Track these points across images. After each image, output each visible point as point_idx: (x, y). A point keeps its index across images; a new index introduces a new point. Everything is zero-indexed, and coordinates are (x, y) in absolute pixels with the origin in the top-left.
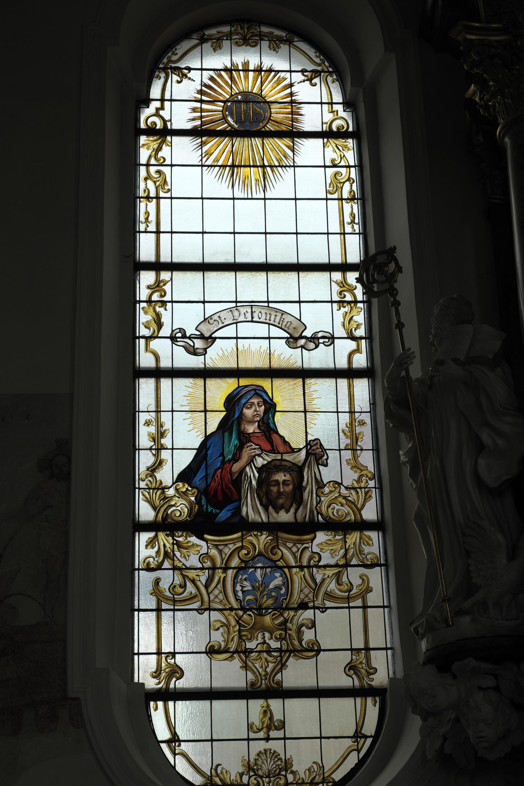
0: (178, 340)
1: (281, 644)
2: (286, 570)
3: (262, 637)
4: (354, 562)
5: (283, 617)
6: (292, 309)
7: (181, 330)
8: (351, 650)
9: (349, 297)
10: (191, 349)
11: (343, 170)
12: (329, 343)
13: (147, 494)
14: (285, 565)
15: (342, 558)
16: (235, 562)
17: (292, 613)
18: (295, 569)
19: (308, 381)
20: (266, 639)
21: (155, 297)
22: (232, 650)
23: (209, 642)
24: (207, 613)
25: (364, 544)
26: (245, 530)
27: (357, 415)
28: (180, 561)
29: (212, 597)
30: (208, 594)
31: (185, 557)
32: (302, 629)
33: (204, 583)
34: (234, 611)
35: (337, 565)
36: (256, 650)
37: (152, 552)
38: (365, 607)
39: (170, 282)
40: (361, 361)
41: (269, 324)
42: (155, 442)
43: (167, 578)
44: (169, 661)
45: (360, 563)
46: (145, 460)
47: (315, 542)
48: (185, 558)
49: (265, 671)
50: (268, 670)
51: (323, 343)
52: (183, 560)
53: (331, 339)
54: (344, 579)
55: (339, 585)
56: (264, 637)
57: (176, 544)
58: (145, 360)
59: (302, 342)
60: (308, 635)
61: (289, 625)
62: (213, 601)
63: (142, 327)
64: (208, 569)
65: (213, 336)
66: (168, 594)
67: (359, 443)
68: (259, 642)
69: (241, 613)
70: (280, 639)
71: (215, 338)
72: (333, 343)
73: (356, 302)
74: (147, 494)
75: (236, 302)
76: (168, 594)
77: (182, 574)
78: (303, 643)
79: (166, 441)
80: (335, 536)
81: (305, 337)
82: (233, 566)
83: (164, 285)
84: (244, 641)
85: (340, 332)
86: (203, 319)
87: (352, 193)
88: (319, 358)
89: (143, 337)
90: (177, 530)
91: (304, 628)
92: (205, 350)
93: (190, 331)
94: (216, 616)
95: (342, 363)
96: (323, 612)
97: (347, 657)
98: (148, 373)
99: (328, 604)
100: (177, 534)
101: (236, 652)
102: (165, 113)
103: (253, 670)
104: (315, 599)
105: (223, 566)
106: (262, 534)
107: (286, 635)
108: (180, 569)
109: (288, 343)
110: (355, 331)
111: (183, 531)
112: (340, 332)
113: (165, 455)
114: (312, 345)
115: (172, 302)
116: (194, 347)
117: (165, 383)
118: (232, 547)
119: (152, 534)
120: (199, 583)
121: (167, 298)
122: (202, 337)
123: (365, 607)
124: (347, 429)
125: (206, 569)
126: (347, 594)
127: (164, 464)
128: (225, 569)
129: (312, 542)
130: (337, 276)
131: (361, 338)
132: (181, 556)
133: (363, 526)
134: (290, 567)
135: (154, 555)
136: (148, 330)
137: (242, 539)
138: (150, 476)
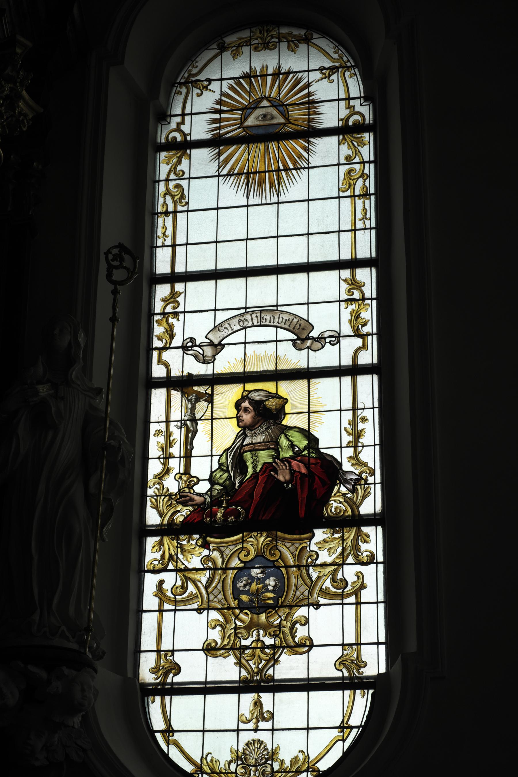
1: (275, 641)
2: (283, 570)
6: (301, 311)
7: (192, 340)
8: (343, 645)
9: (357, 295)
11: (357, 167)
13: (153, 500)
14: (283, 565)
16: (235, 563)
19: (313, 381)
20: (261, 636)
21: (169, 309)
23: (206, 640)
24: (206, 612)
27: (359, 412)
28: (183, 564)
29: (211, 597)
30: (208, 594)
31: (187, 559)
33: (204, 583)
38: (358, 603)
40: (367, 358)
42: (163, 451)
43: (170, 579)
46: (154, 467)
47: (314, 541)
49: (258, 667)
50: (260, 666)
51: (330, 342)
52: (186, 563)
54: (340, 576)
56: (258, 635)
57: (180, 547)
58: (158, 371)
60: (301, 632)
62: (212, 601)
63: (155, 339)
64: (209, 569)
65: (222, 343)
66: (169, 594)
67: (360, 440)
68: (254, 639)
69: (237, 611)
71: (224, 345)
72: (339, 341)
73: (364, 299)
76: (169, 594)
78: (296, 640)
80: (333, 535)
84: (239, 638)
86: (213, 327)
87: (365, 189)
88: (326, 357)
89: (156, 349)
90: (181, 535)
91: (298, 626)
92: (214, 357)
94: (214, 615)
95: (347, 361)
100: (181, 538)
102: (185, 128)
103: (246, 668)
104: (310, 597)
105: (224, 567)
107: (280, 632)
109: (294, 345)
110: (362, 327)
112: (347, 330)
114: (318, 345)
115: (185, 312)
116: (203, 355)
118: (233, 548)
119: (158, 539)
120: (199, 584)
121: (181, 309)
122: (211, 344)
123: (358, 603)
124: (349, 426)
126: (341, 591)
127: (171, 471)
128: (225, 570)
129: (310, 542)
130: (346, 274)
132: (183, 558)
134: (287, 567)
135: (159, 558)
138: (158, 483)
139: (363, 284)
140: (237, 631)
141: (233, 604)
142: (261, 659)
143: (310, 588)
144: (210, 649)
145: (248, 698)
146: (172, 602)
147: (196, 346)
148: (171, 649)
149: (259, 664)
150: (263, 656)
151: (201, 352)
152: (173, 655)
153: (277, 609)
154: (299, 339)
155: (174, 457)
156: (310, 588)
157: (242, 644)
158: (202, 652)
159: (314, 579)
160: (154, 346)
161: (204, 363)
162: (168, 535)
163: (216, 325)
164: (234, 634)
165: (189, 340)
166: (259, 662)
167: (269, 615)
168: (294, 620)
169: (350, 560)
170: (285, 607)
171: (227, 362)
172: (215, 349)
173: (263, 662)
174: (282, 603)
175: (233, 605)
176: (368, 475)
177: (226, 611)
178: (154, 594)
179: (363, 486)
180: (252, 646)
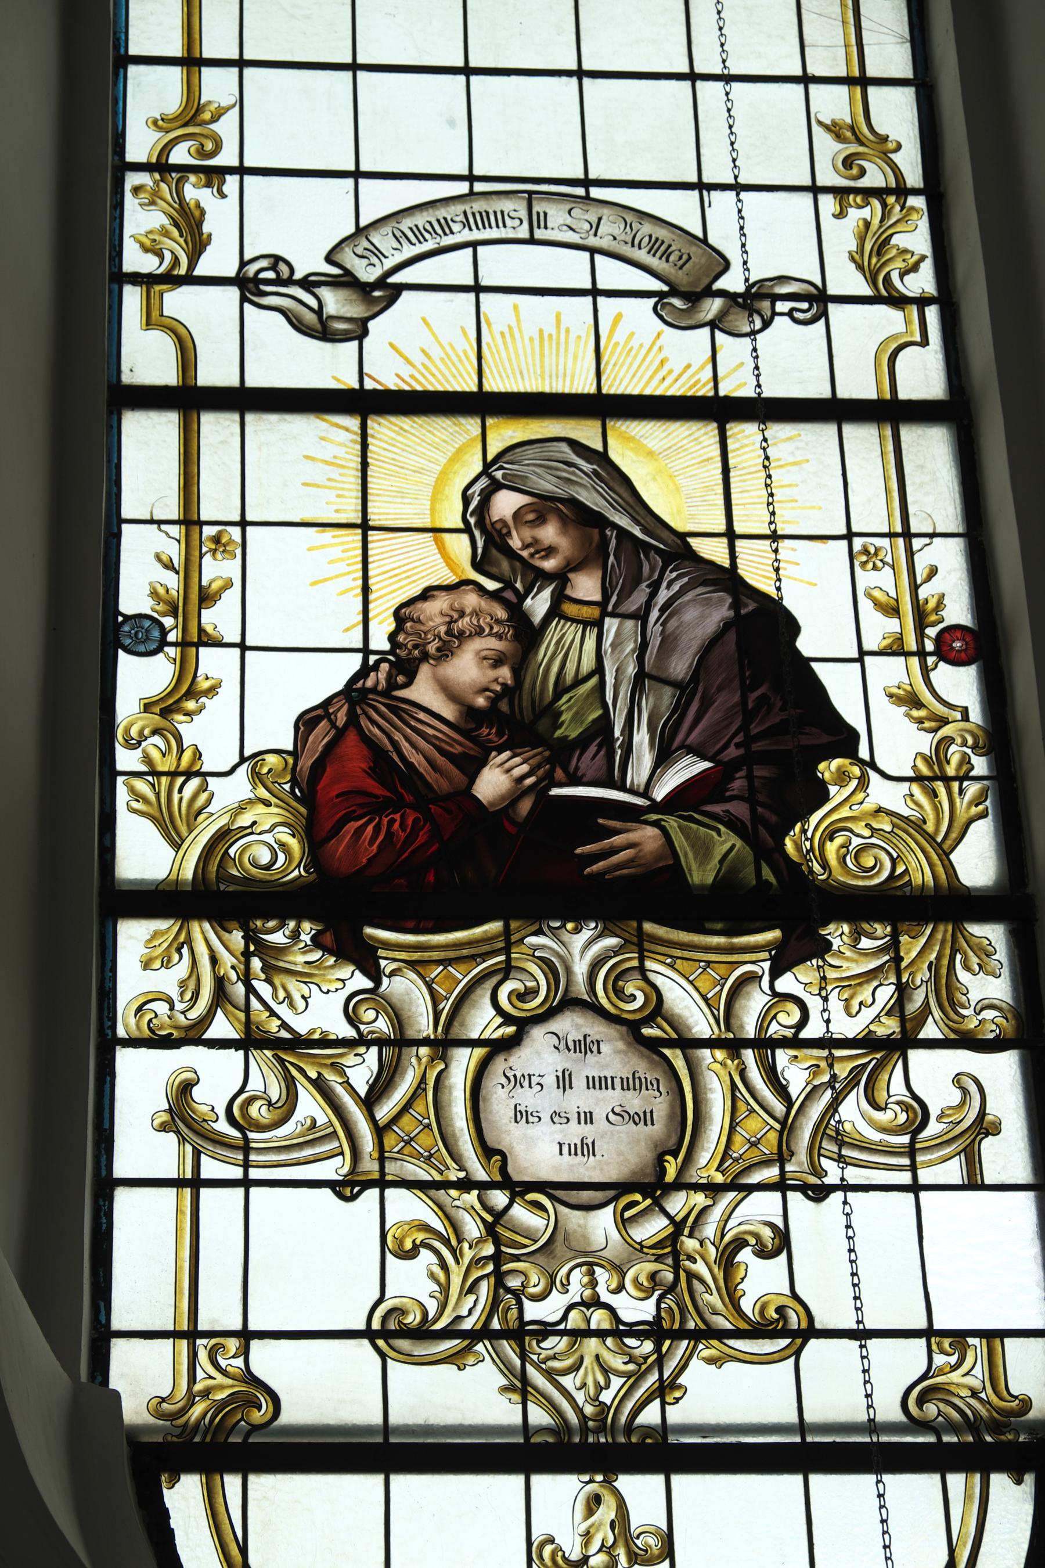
3: (586, 1280)
4: (930, 1031)
6: (679, 209)
9: (875, 177)
10: (310, 318)
12: (808, 315)
16: (482, 1021)
17: (700, 1199)
18: (706, 1053)
21: (180, 155)
24: (372, 1195)
30: (380, 1131)
32: (739, 1258)
33: (362, 1090)
34: (475, 1192)
35: (867, 1042)
36: (562, 1327)
39: (237, 107)
41: (593, 251)
44: (223, 1363)
45: (953, 1036)
48: (292, 1005)
51: (790, 314)
53: (818, 301)
55: (877, 1107)
56: (593, 1283)
59: (713, 307)
61: (690, 1244)
64: (381, 1042)
65: (390, 280)
66: (223, 1126)
71: (400, 289)
72: (824, 314)
73: (902, 191)
76: (223, 1126)
79: (221, 618)
81: (722, 293)
82: (474, 1035)
83: (215, 119)
85: (846, 279)
86: (352, 229)
89: (136, 278)
91: (745, 1255)
93: (309, 261)
94: (406, 1207)
96: (818, 1200)
98: (152, 398)
101: (483, 1333)
106: (577, 931)
110: (902, 276)
112: (846, 279)
115: (242, 170)
116: (319, 312)
117: (217, 429)
121: (227, 158)
125: (368, 1044)
126: (906, 1139)
128: (443, 1045)
131: (922, 302)
133: (953, 905)
134: (688, 1044)
135: (174, 993)
136: (156, 260)
137: (508, 943)
140: (505, 1268)
142: (606, 1371)
143: (783, 1123)
144: (392, 1333)
147: (289, 282)
149: (600, 1389)
150: (617, 1362)
151: (313, 303)
152: (245, 1352)
154: (674, 292)
155: (220, 644)
157: (528, 1317)
158: (366, 1342)
160: (128, 267)
162: (200, 916)
163: (363, 223)
165: (264, 263)
167: (627, 1215)
169: (930, 1031)
170: (696, 1187)
171: (414, 343)
173: (616, 1382)
175: (481, 1175)
176: (969, 751)
177: (454, 1193)
179: (955, 785)
180: (570, 1325)
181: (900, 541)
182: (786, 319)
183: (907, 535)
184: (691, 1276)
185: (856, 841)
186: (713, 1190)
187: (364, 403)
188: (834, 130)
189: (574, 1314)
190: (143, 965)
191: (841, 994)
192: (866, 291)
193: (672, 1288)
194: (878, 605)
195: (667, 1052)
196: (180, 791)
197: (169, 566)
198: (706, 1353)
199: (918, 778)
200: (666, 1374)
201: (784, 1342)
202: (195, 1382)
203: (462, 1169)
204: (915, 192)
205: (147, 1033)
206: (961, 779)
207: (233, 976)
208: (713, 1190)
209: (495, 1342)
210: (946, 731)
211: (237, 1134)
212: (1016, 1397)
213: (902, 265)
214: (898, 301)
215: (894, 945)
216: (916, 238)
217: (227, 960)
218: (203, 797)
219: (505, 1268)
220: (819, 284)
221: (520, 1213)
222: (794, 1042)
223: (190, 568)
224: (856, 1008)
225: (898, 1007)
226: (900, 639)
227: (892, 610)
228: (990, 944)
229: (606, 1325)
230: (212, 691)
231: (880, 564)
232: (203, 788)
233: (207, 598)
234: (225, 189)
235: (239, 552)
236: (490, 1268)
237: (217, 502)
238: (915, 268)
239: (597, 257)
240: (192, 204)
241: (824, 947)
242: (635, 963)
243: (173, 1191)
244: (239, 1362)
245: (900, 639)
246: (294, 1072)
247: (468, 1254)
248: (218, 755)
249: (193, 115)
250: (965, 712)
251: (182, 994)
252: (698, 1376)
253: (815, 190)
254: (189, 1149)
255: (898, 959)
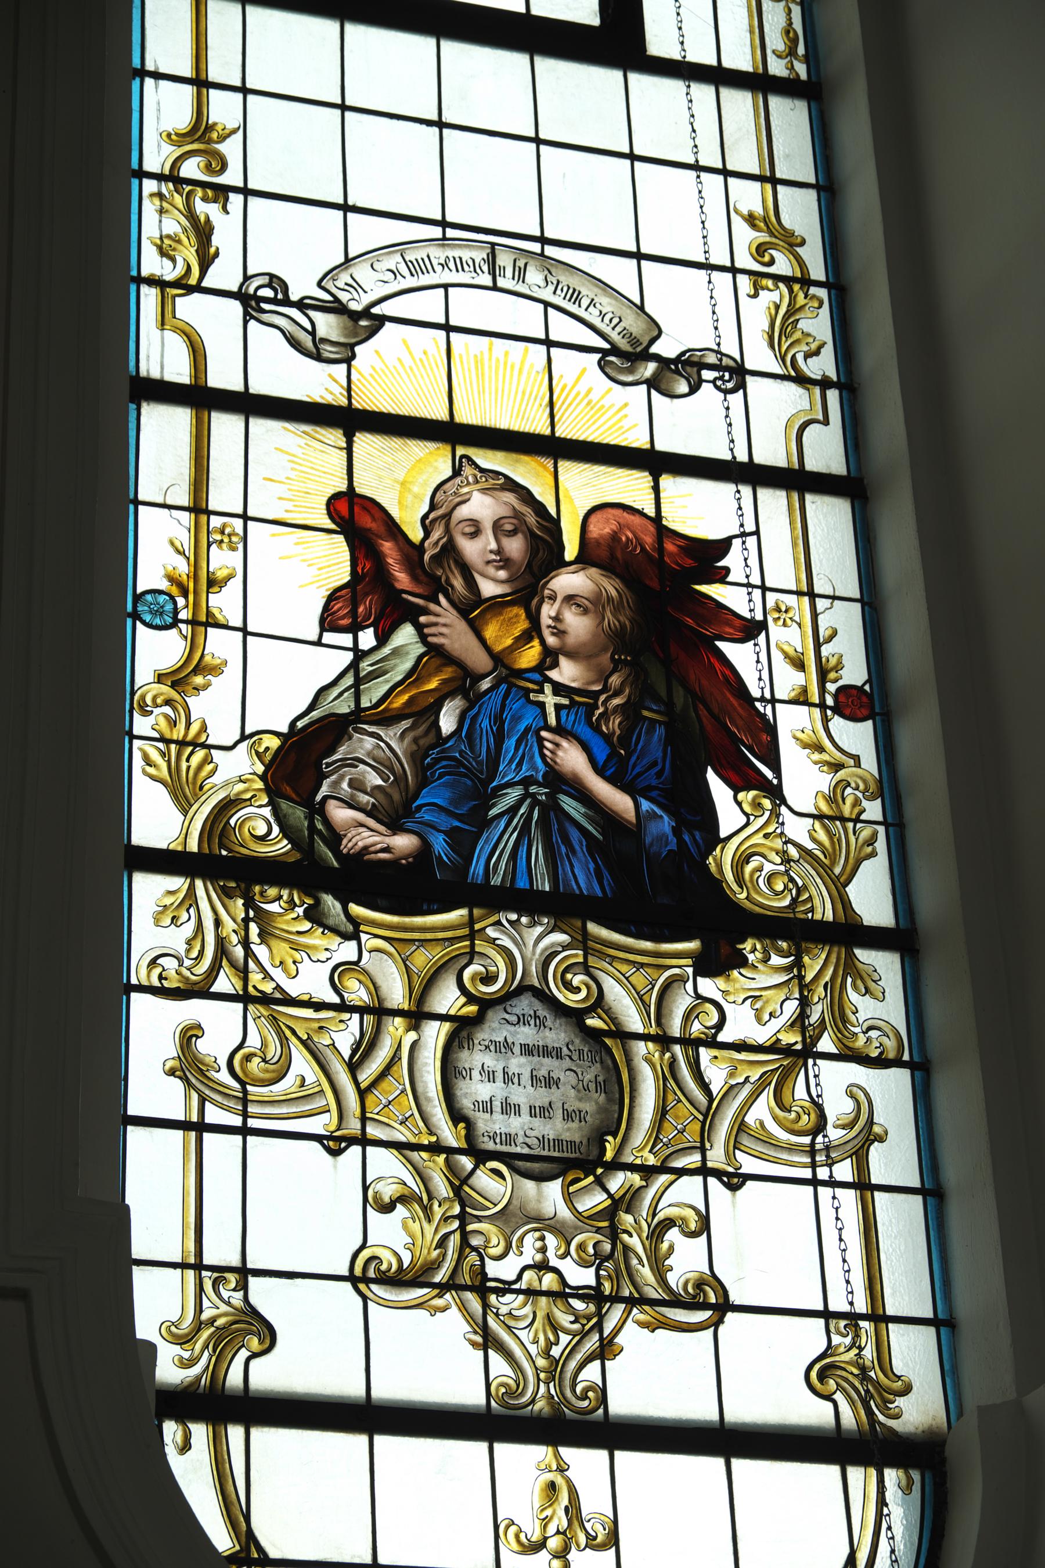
0: (263, 305)
1: (598, 1277)
5: (607, 1191)
7: (274, 281)
8: (826, 1314)
9: (783, 265)
12: (730, 385)
13: (155, 756)
15: (792, 1025)
17: (636, 1179)
20: (551, 1254)
21: (191, 169)
22: (437, 1279)
23: (363, 1246)
24: (356, 1150)
25: (855, 987)
26: (479, 905)
30: (362, 1094)
33: (346, 1054)
34: (444, 1156)
36: (516, 1286)
37: (176, 938)
38: (863, 1186)
41: (547, 304)
43: (221, 1027)
48: (286, 971)
51: (714, 382)
53: (736, 375)
54: (800, 1092)
61: (627, 1219)
64: (362, 1010)
66: (224, 1076)
69: (466, 1162)
70: (599, 1260)
71: (381, 320)
72: (742, 386)
73: (806, 282)
74: (155, 756)
75: (444, 224)
77: (274, 1020)
78: (672, 1278)
79: (225, 603)
81: (657, 358)
82: (443, 1011)
83: (222, 139)
85: (759, 356)
89: (153, 281)
91: (673, 1235)
97: (810, 1338)
98: (165, 392)
99: (749, 1165)
104: (708, 1145)
106: (533, 924)
108: (265, 1000)
111: (281, 884)
112: (759, 356)
113: (220, 644)
116: (313, 333)
121: (232, 177)
122: (337, 308)
131: (825, 384)
133: (848, 933)
134: (626, 1037)
139: (799, 240)
141: (450, 1135)
143: (706, 1116)
145: (523, 1462)
146: (227, 1102)
147: (287, 302)
148: (235, 1261)
149: (550, 1345)
153: (599, 1171)
156: (706, 1116)
159: (715, 1088)
161: (318, 357)
164: (458, 1235)
165: (265, 280)
166: (552, 1338)
168: (661, 1216)
170: (632, 1168)
171: (394, 372)
172: (350, 323)
173: (564, 1339)
174: (619, 1151)
176: (860, 795)
177: (424, 1155)
178: (170, 1064)
179: (850, 825)
180: (523, 1285)
181: (806, 599)
182: (711, 385)
183: (812, 595)
184: (627, 1248)
185: (768, 867)
186: (648, 1172)
187: (349, 420)
188: (751, 219)
189: (528, 1275)
190: (157, 920)
191: (751, 1004)
192: (778, 370)
193: (610, 1257)
194: (786, 656)
195: (608, 1041)
196: (188, 760)
197: (182, 553)
198: (642, 1317)
199: (819, 817)
200: (606, 1333)
201: (708, 1314)
202: (201, 1311)
203: (431, 1133)
204: (818, 284)
205: (156, 983)
206: (857, 820)
207: (234, 939)
208: (648, 1172)
209: (460, 1292)
210: (841, 775)
211: (236, 1085)
212: (899, 1377)
213: (805, 348)
214: (801, 380)
215: (798, 964)
216: (818, 325)
217: (229, 925)
218: (209, 768)
219: (470, 1228)
220: (738, 357)
221: (483, 1180)
222: (712, 1043)
223: (197, 558)
224: (766, 1017)
225: (800, 1021)
226: (805, 690)
227: (799, 664)
228: (875, 971)
229: (556, 1287)
230: (216, 670)
231: (789, 622)
232: (207, 760)
233: (214, 583)
234: (229, 207)
235: (241, 546)
236: (456, 1224)
237: (223, 496)
238: (817, 353)
239: (550, 309)
240: (202, 219)
241: (741, 962)
242: (581, 960)
243: (179, 1134)
244: (240, 1295)
245: (805, 690)
246: (288, 1033)
247: (438, 1211)
248: (223, 731)
249: (200, 134)
250: (857, 759)
251: (188, 951)
252: (633, 1337)
253: (733, 270)
254: (195, 1096)
255: (801, 977)
